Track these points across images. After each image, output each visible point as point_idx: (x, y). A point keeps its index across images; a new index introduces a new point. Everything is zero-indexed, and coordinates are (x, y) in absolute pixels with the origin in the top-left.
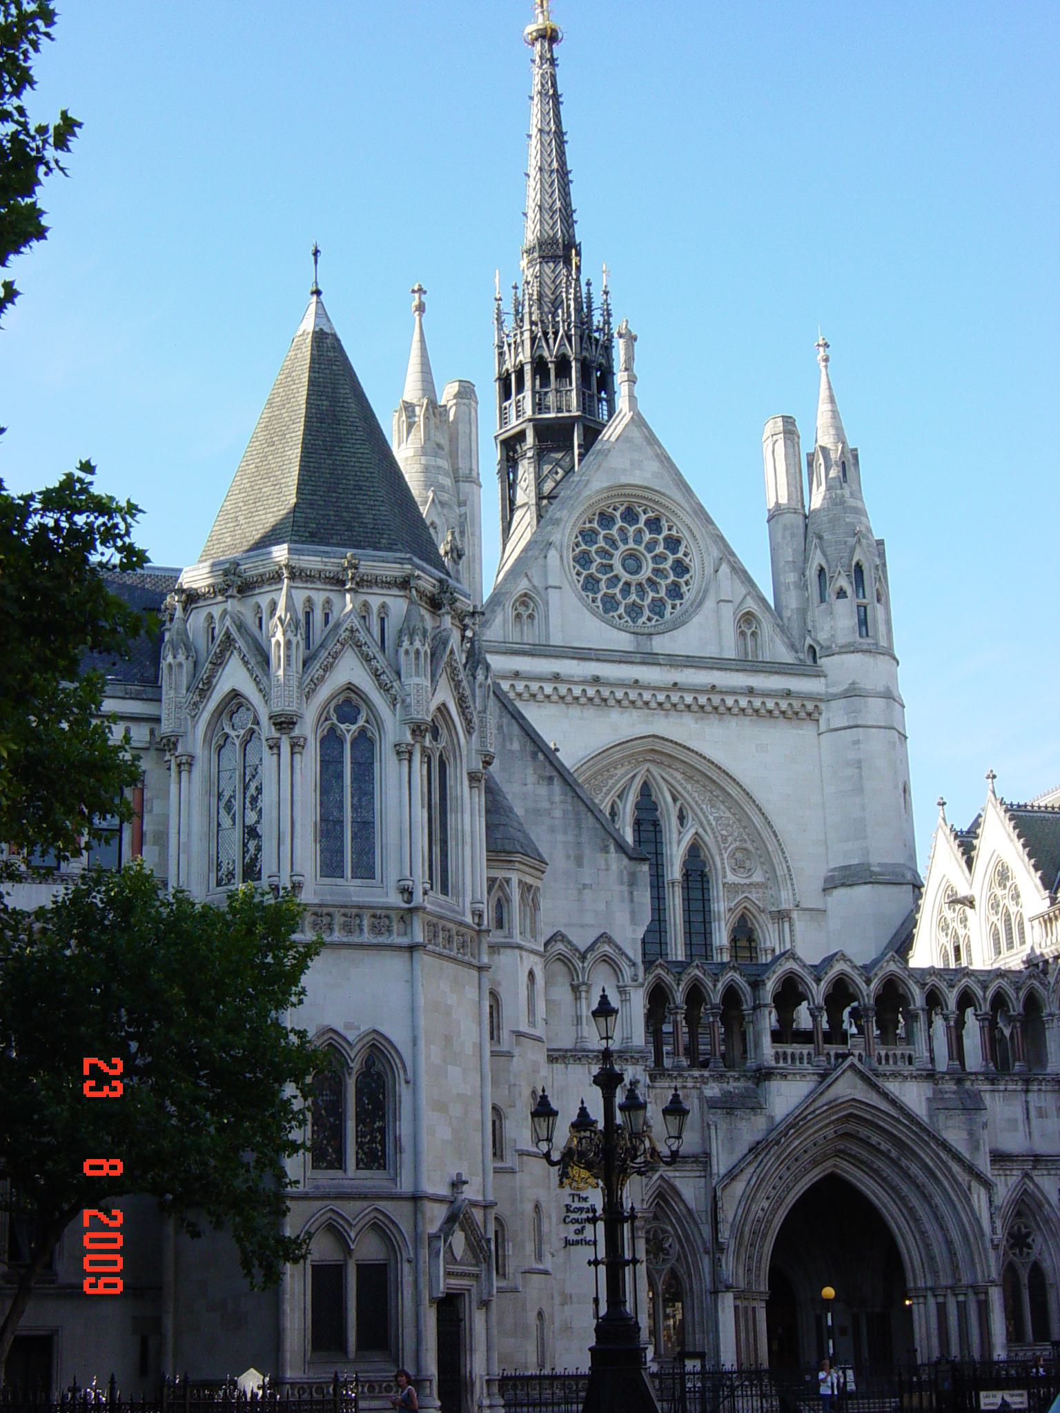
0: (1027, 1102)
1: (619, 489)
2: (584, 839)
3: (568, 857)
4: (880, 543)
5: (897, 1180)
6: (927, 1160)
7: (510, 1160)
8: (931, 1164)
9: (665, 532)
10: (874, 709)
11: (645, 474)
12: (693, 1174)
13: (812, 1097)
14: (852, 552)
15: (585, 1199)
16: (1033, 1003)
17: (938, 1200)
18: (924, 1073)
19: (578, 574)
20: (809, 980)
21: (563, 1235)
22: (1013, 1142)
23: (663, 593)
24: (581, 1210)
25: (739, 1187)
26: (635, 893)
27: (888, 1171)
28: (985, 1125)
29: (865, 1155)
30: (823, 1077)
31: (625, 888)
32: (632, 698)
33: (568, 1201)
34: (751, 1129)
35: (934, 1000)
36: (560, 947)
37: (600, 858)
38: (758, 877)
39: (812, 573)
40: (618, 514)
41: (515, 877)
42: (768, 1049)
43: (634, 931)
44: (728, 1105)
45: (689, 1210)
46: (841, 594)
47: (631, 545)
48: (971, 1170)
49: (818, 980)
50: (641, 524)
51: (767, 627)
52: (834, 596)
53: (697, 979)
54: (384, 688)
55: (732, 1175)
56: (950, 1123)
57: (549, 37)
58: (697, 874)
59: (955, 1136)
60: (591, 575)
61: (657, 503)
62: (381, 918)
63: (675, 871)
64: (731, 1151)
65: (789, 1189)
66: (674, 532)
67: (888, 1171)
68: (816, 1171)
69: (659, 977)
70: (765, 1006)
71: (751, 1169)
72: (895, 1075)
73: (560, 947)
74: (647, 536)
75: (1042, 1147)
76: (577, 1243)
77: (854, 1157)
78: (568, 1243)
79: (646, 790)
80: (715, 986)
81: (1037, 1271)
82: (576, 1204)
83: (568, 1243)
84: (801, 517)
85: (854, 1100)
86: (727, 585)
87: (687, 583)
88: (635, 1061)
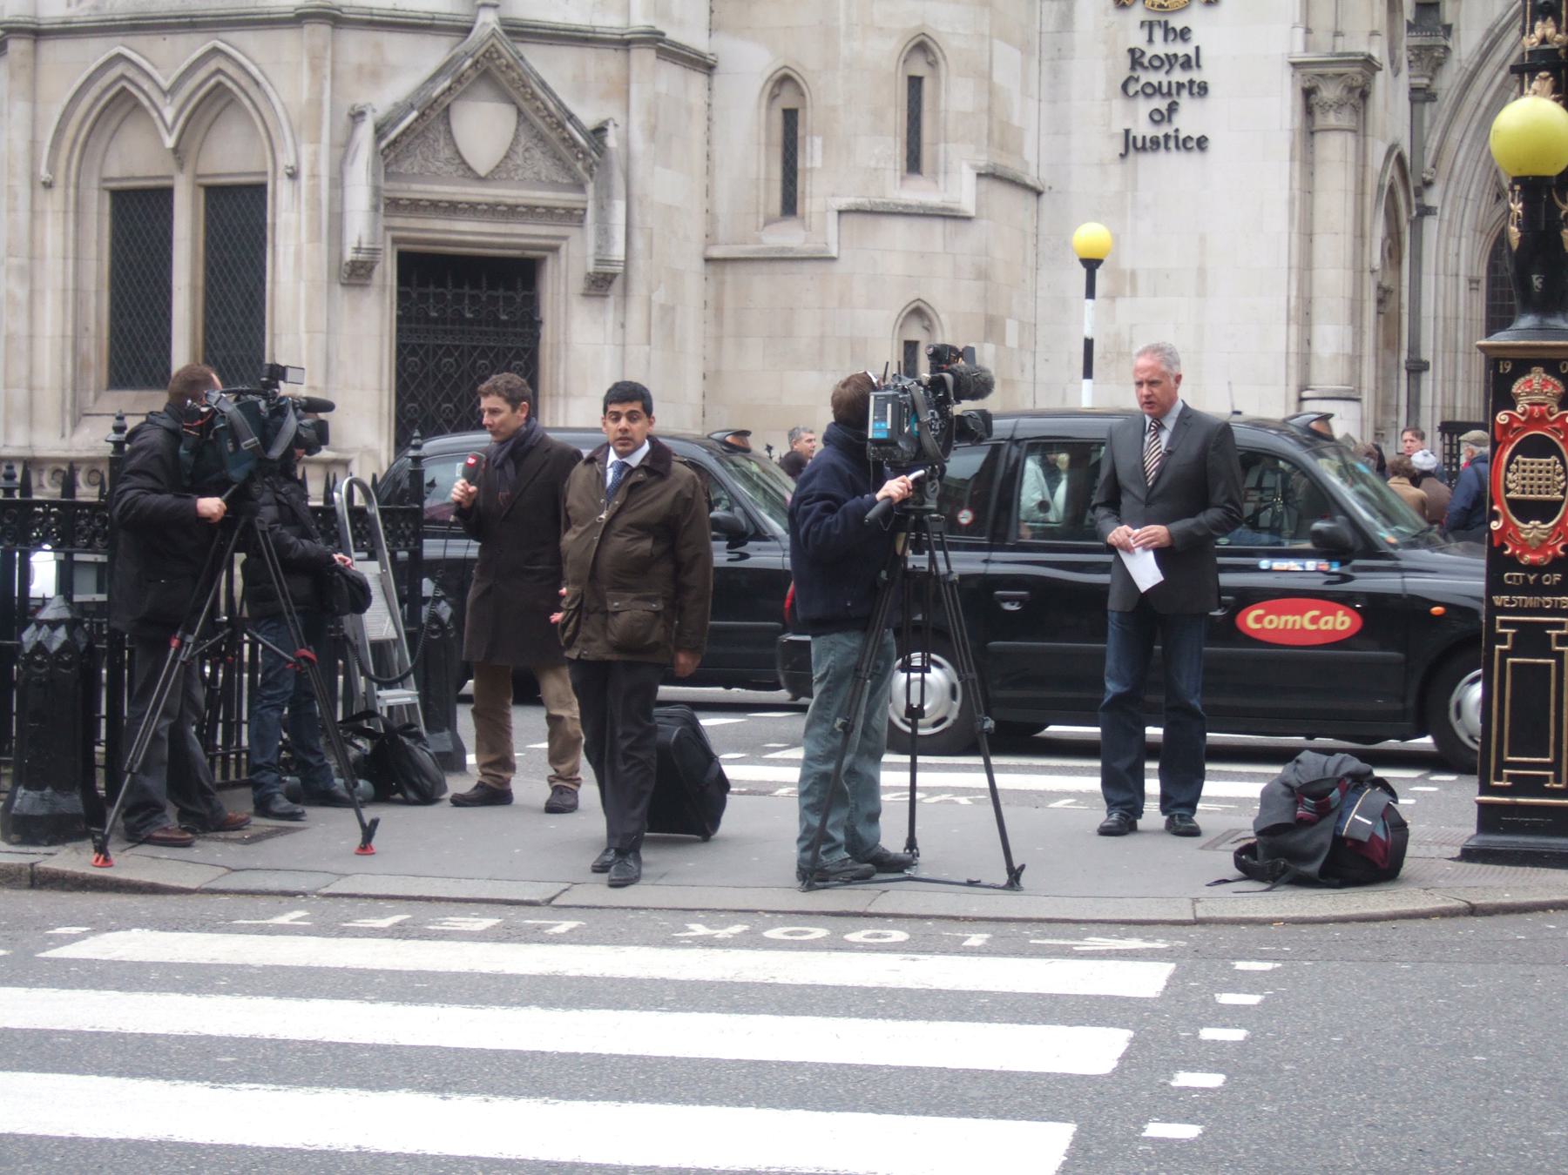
15: (1184, 34)
21: (1119, 129)
24: (1171, 60)
33: (1138, 39)
76: (1155, 142)
78: (1132, 145)
82: (1160, 48)
83: (1132, 145)
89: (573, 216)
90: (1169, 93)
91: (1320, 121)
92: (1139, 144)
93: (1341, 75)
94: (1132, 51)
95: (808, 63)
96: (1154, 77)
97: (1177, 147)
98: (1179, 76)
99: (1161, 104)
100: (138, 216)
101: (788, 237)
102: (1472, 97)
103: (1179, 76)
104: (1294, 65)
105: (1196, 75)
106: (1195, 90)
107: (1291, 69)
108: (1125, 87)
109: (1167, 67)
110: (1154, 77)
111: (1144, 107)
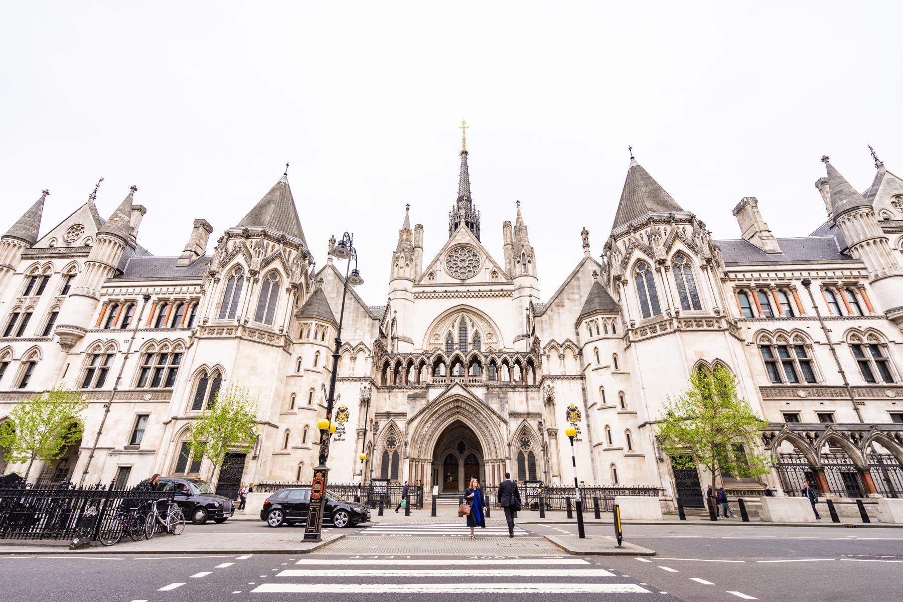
5: (477, 421)
7: (296, 410)
10: (527, 292)
13: (443, 395)
16: (530, 362)
17: (490, 428)
22: (522, 409)
25: (415, 423)
27: (474, 418)
28: (507, 402)
32: (457, 295)
34: (421, 404)
35: (493, 362)
36: (347, 346)
37: (363, 320)
38: (495, 341)
41: (314, 322)
44: (413, 397)
46: (519, 262)
48: (499, 417)
51: (500, 275)
54: (247, 262)
58: (477, 341)
62: (230, 329)
63: (470, 339)
67: (474, 418)
73: (347, 346)
75: (532, 410)
79: (463, 321)
81: (531, 454)
83: (335, 440)
88: (366, 381)
89: (252, 448)
95: (291, 427)
100: (185, 447)
101: (285, 451)
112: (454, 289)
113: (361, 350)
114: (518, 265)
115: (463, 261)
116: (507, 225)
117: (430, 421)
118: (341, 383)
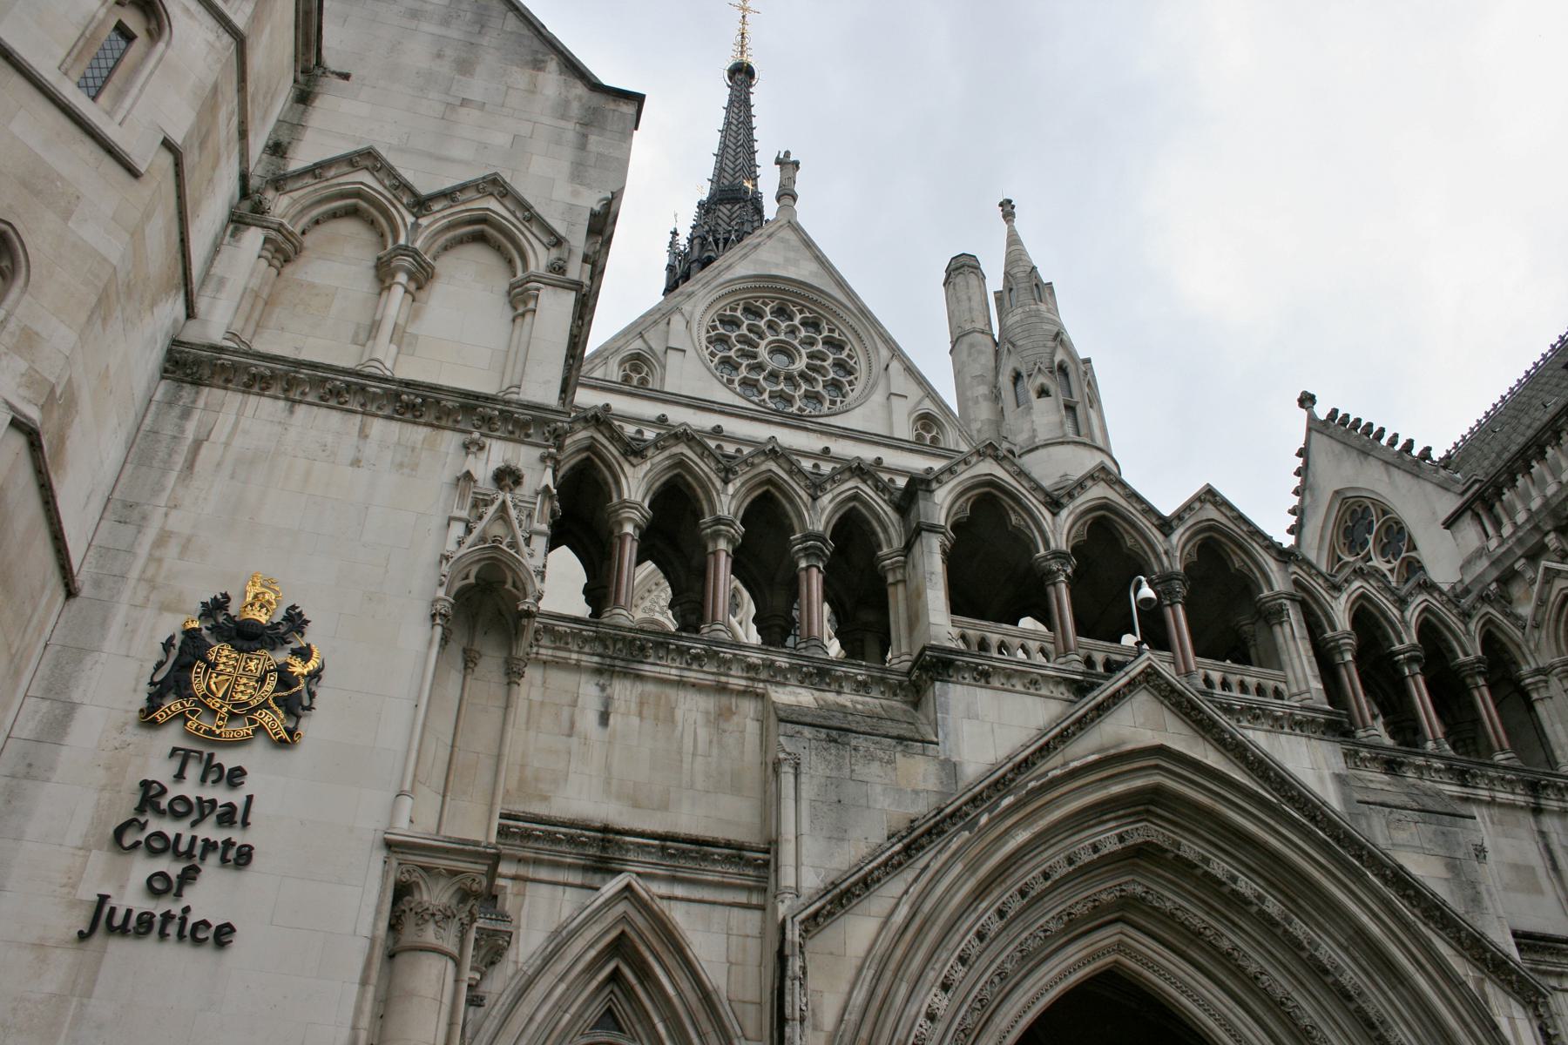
0: (1543, 834)
1: (768, 283)
2: (485, 41)
3: (439, 56)
4: (1088, 361)
6: (1365, 919)
8: (1374, 929)
9: (826, 333)
11: (804, 271)
12: (729, 896)
14: (1053, 354)
15: (235, 777)
18: (1321, 718)
19: (712, 354)
20: (1034, 502)
23: (819, 388)
24: (204, 808)
25: (859, 931)
26: (593, 138)
29: (1197, 916)
30: (1081, 689)
31: (570, 126)
33: (161, 771)
34: (899, 789)
39: (1005, 380)
40: (768, 309)
42: (940, 623)
43: (575, 194)
45: (706, 996)
46: (1043, 392)
47: (782, 337)
49: (1055, 505)
50: (796, 322)
52: (1033, 395)
53: (771, 481)
55: (842, 897)
56: (1401, 836)
57: (742, 74)
59: (1425, 869)
60: (726, 361)
61: (815, 302)
64: (838, 835)
65: (1006, 982)
66: (836, 335)
68: (1075, 953)
69: (681, 463)
70: (933, 529)
71: (894, 887)
72: (1255, 714)
74: (803, 333)
76: (144, 926)
77: (1168, 918)
78: (104, 922)
80: (815, 499)
82: (191, 789)
83: (104, 922)
84: (991, 344)
85: (1161, 751)
86: (900, 381)
87: (850, 383)
90: (189, 854)
91: (409, 935)
92: (118, 921)
93: (453, 873)
94: (146, 785)
96: (170, 828)
97: (181, 936)
98: (209, 831)
99: (174, 869)
102: (524, 1010)
103: (209, 831)
104: (390, 845)
105: (238, 837)
106: (232, 854)
107: (382, 854)
108: (119, 833)
109: (195, 816)
110: (170, 828)
111: (142, 868)
112: (761, 432)
113: (482, 233)
114: (1040, 405)
115: (780, 349)
116: (962, 268)
117: (964, 938)
118: (266, 408)
